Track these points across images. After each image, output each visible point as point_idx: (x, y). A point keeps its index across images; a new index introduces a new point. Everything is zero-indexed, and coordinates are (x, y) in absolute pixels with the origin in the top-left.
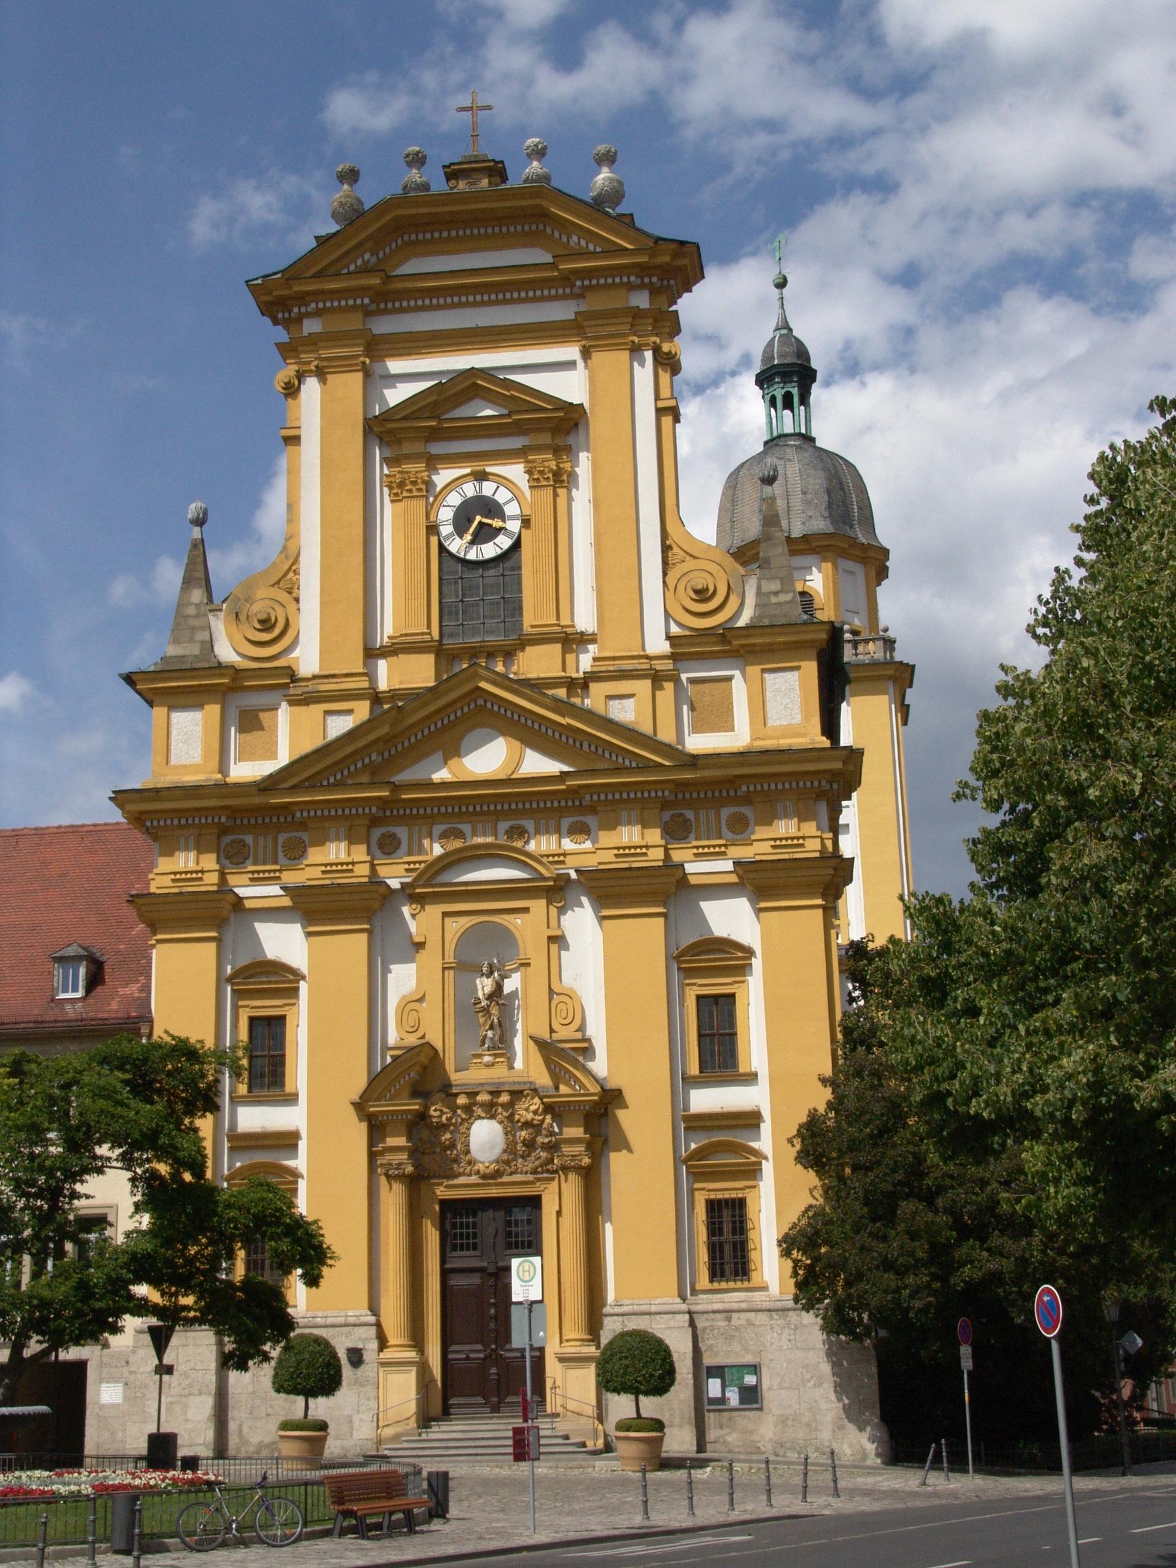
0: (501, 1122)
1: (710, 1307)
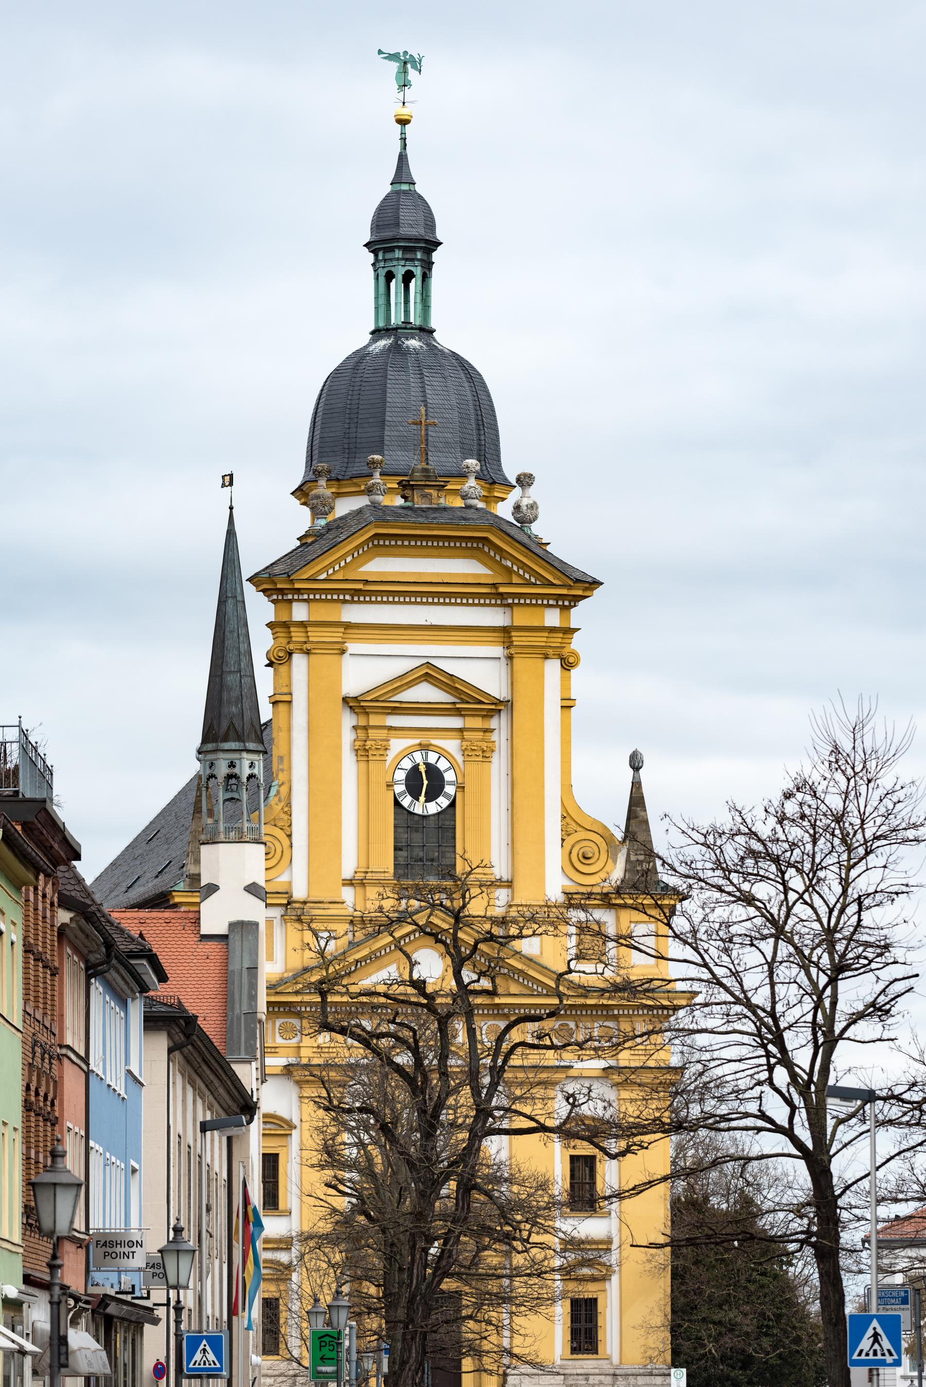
1: (575, 1372)
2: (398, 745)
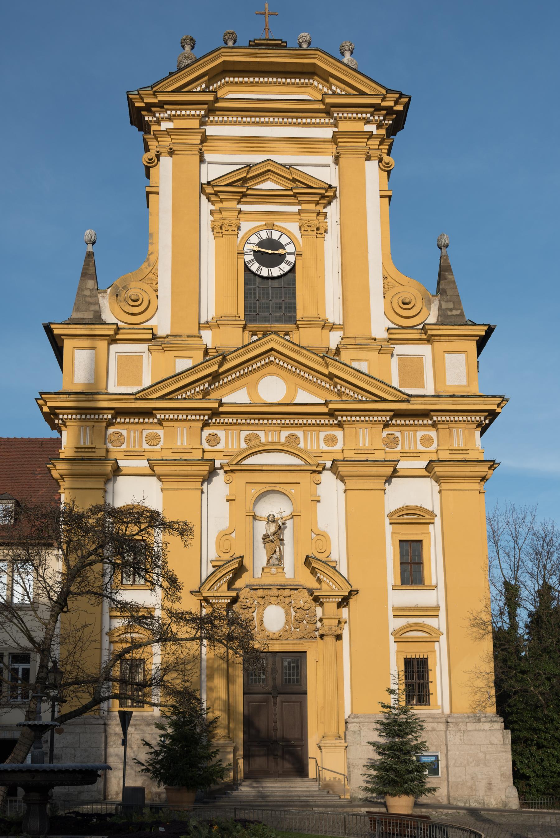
0: (284, 608)
2: (246, 226)
